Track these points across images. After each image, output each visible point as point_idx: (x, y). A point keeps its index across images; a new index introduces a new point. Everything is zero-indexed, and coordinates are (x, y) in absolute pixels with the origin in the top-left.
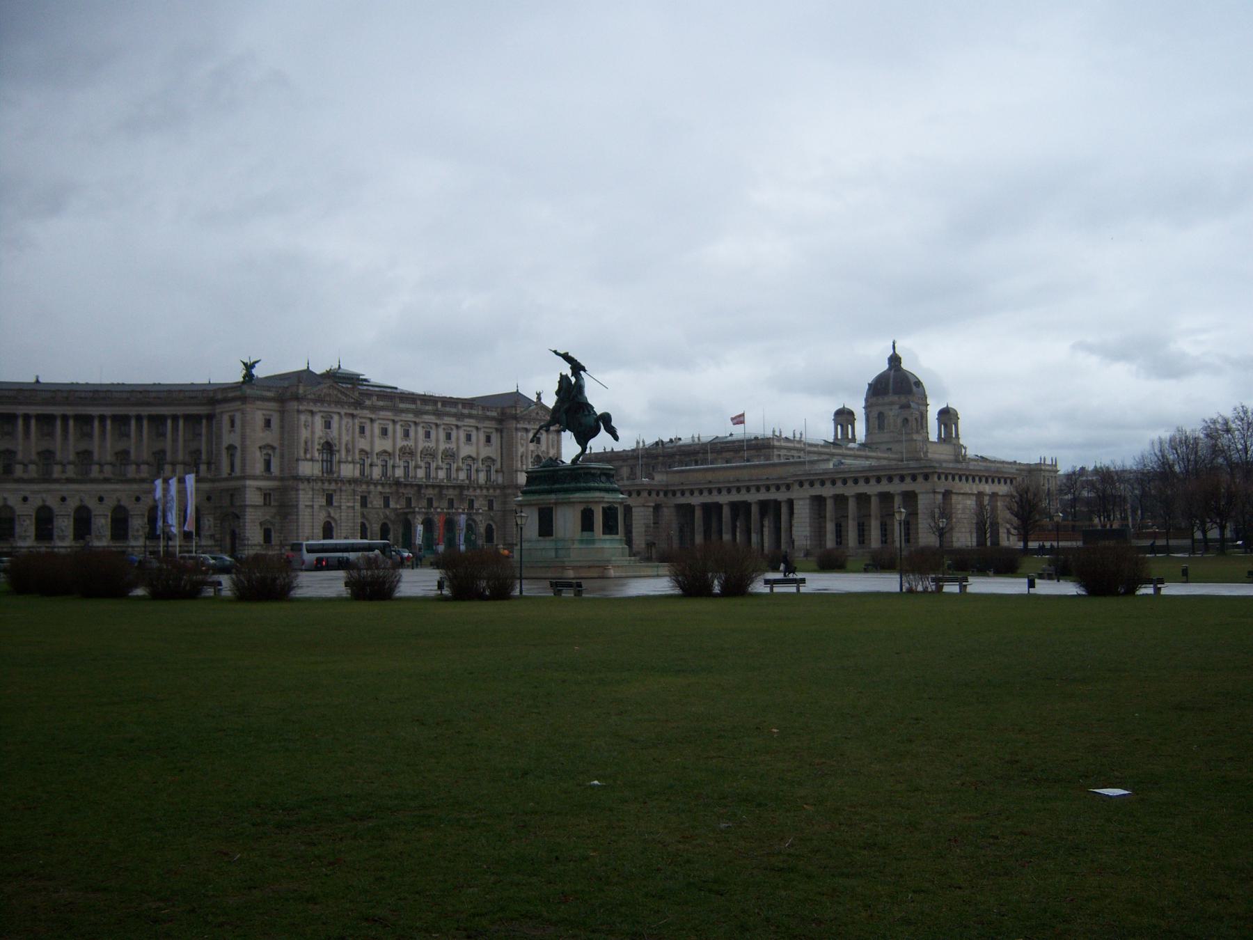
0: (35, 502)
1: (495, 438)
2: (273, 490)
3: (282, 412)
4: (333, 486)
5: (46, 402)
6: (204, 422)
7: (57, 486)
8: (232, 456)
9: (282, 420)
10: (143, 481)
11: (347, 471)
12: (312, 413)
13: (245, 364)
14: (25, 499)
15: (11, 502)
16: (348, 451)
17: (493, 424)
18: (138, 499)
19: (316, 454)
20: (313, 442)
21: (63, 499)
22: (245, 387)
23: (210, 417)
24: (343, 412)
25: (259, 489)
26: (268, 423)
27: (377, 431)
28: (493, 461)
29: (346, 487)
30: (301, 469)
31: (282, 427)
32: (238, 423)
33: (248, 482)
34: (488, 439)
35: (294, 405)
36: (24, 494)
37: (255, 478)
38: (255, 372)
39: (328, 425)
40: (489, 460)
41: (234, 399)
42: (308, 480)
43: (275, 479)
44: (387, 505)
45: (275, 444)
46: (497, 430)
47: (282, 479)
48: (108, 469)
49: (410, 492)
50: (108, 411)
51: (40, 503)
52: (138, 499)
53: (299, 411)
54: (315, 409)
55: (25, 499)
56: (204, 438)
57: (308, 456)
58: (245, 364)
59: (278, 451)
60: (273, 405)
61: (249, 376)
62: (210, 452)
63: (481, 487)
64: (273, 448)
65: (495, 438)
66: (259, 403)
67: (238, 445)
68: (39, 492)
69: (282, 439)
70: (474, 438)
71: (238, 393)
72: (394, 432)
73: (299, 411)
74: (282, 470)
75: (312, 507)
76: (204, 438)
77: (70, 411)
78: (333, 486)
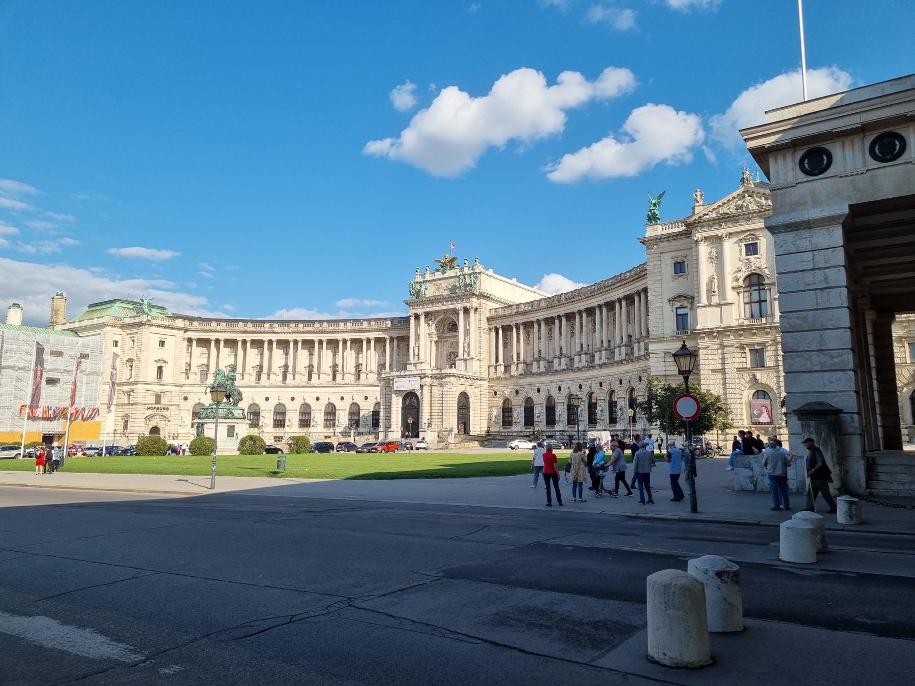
0: (586, 390)
7: (595, 372)
10: (639, 358)
14: (580, 387)
18: (640, 379)
19: (731, 296)
21: (601, 385)
30: (700, 318)
36: (580, 382)
37: (659, 340)
39: (752, 249)
42: (710, 333)
52: (640, 379)
53: (697, 242)
54: (720, 232)
55: (580, 387)
75: (723, 371)
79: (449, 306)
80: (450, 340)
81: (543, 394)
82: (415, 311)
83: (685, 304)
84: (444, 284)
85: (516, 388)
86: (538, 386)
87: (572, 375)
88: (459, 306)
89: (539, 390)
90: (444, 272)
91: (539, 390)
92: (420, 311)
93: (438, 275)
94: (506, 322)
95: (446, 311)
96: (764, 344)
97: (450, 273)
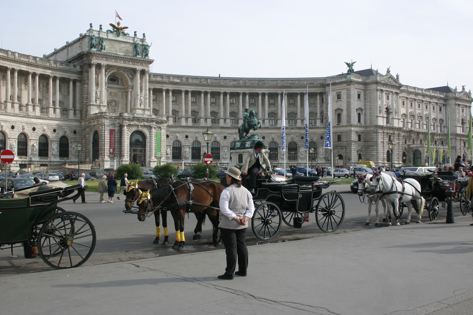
1: (443, 109)
2: (362, 133)
3: (365, 91)
4: (391, 132)
5: (235, 86)
6: (318, 96)
8: (339, 116)
9: (365, 95)
11: (397, 124)
12: (382, 91)
13: (347, 64)
14: (225, 137)
15: (218, 139)
16: (396, 113)
17: (442, 102)
20: (383, 107)
22: (348, 76)
23: (322, 94)
24: (394, 91)
25: (357, 132)
26: (359, 96)
27: (401, 103)
28: (443, 121)
29: (396, 132)
31: (365, 99)
32: (344, 95)
33: (352, 129)
34: (440, 110)
35: (374, 87)
38: (353, 67)
40: (441, 120)
41: (341, 83)
43: (361, 127)
44: (406, 142)
45: (363, 108)
46: (444, 105)
47: (366, 127)
48: (267, 121)
49: (414, 136)
50: (266, 91)
51: (233, 140)
53: (377, 90)
54: (384, 89)
55: (225, 137)
56: (318, 106)
57: (381, 114)
58: (347, 64)
59: (363, 111)
60: (361, 87)
61: (351, 71)
62: (322, 113)
63: (439, 135)
64: (362, 110)
65: (443, 109)
66: (356, 85)
67: (344, 107)
68: (232, 134)
69: (365, 105)
70: (435, 109)
71: (344, 80)
72: (407, 104)
73: (377, 90)
74: (365, 122)
76: (318, 106)
77: (247, 90)
78: (391, 132)
79: (131, 66)
80: (111, 90)
81: (191, 140)
82: (99, 62)
83: (361, 112)
84: (117, 45)
85: (168, 133)
86: (186, 134)
87: (218, 130)
88: (139, 67)
89: (187, 137)
90: (118, 36)
91: (187, 137)
92: (104, 62)
93: (111, 36)
94: (158, 86)
95: (119, 68)
96: (392, 134)
97: (121, 38)
